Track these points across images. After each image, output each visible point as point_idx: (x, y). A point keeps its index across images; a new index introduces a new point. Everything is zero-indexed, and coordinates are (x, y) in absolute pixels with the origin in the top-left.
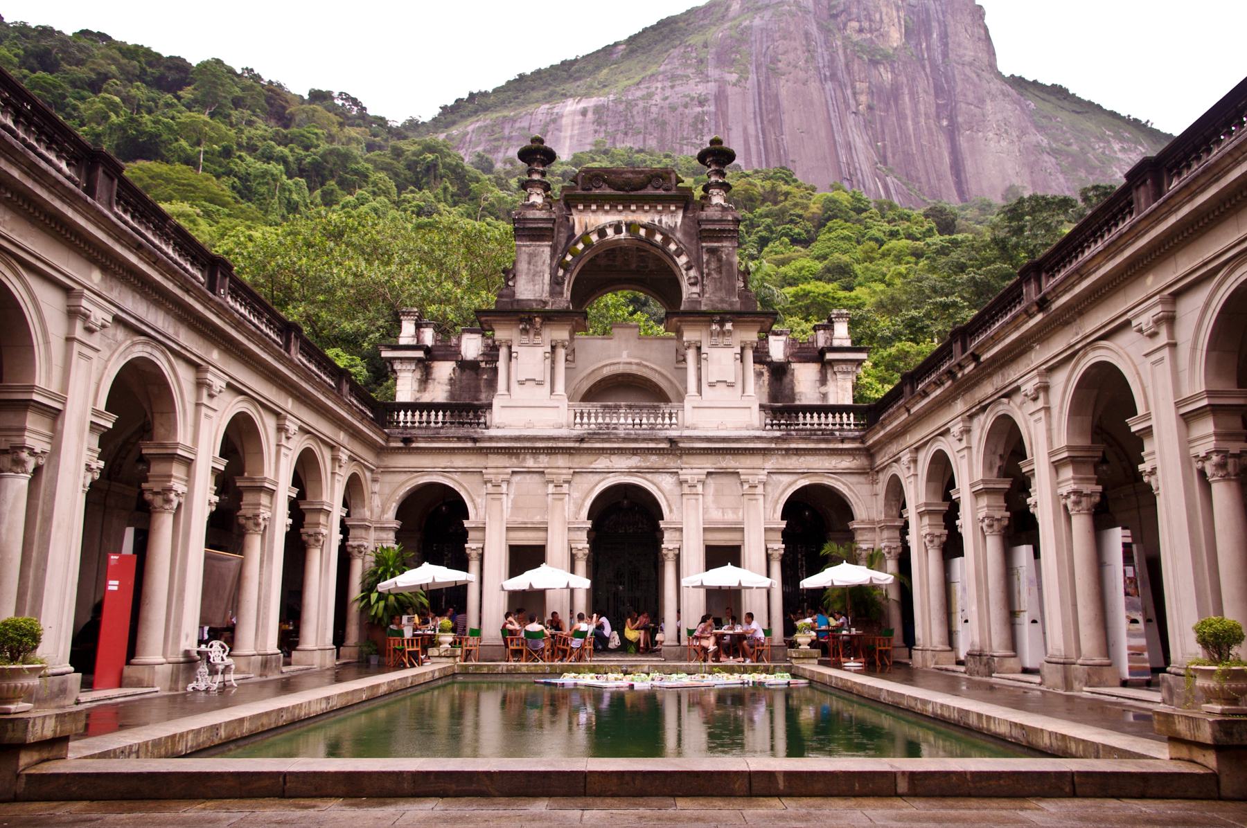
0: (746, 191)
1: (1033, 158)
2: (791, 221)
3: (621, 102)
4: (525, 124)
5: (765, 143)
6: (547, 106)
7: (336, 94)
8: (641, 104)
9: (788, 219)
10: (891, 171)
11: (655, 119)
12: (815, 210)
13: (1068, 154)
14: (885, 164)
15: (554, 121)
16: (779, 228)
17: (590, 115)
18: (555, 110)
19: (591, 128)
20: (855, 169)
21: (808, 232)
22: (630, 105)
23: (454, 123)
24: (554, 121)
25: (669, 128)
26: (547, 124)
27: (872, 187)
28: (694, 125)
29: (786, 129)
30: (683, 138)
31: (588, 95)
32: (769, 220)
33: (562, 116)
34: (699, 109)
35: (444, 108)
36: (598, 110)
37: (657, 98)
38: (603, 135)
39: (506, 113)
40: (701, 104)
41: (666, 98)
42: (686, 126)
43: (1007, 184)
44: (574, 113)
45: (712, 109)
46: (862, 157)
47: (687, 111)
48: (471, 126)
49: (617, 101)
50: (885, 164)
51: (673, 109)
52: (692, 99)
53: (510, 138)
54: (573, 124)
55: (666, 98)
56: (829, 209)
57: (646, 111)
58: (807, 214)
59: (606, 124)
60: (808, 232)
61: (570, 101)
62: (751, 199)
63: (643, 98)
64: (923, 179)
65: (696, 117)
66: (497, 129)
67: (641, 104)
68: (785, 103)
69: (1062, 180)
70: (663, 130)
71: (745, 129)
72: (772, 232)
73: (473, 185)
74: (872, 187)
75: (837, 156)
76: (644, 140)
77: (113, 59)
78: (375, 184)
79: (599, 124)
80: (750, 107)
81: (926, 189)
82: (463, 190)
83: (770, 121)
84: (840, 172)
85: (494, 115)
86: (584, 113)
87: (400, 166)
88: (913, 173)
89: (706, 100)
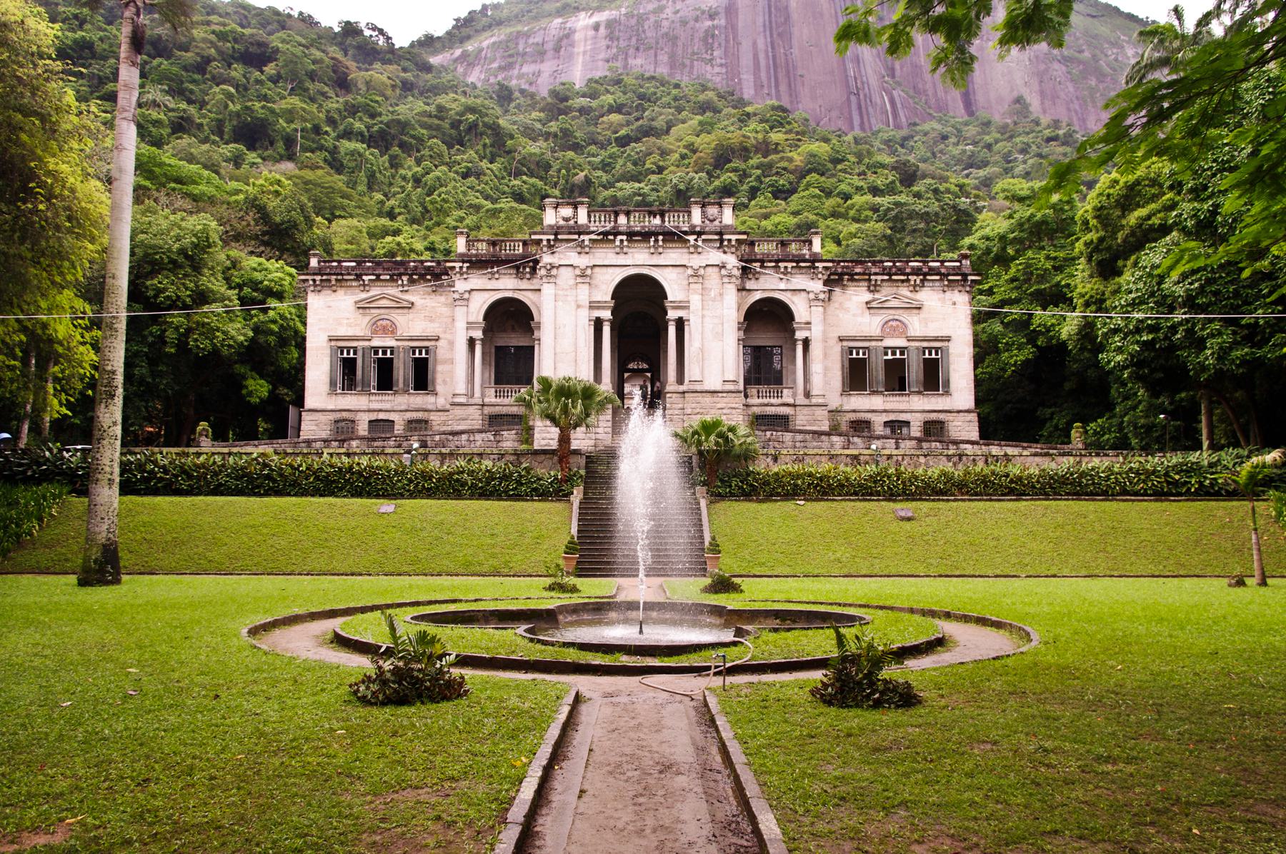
0: (741, 143)
1: (1042, 67)
2: (777, 173)
3: (633, 16)
4: (538, 39)
5: (774, 57)
6: (560, 20)
7: (362, 25)
8: (652, 19)
9: (774, 171)
10: (899, 84)
11: (667, 34)
12: (798, 163)
13: (1080, 62)
14: (893, 76)
15: (567, 36)
16: (767, 179)
17: (602, 30)
18: (568, 25)
19: (604, 43)
20: (863, 83)
21: (791, 183)
22: (641, 19)
23: (469, 37)
24: (567, 36)
25: (680, 43)
26: (560, 40)
27: (878, 101)
28: (705, 40)
29: (795, 42)
30: (694, 53)
31: (599, 9)
32: (759, 172)
33: (575, 31)
34: (709, 23)
35: (457, 20)
36: (610, 24)
37: (669, 11)
38: (615, 50)
39: (519, 28)
40: (712, 17)
41: (677, 12)
42: (696, 40)
43: (1015, 94)
44: (586, 28)
45: (723, 22)
46: (870, 71)
47: (697, 25)
48: (486, 41)
49: (629, 16)
50: (893, 76)
51: (684, 23)
52: (703, 12)
53: (525, 54)
54: (586, 40)
55: (677, 12)
56: (809, 163)
57: (658, 25)
58: (791, 167)
59: (618, 39)
60: (791, 183)
61: (582, 15)
62: (746, 149)
63: (655, 12)
64: (930, 93)
65: (706, 31)
66: (511, 45)
67: (652, 19)
68: (795, 16)
69: (1071, 89)
70: (674, 45)
71: (755, 43)
72: (761, 182)
73: (509, 142)
74: (878, 101)
75: (845, 70)
76: (656, 56)
77: (211, 42)
78: (431, 149)
79: (611, 39)
80: (760, 21)
81: (933, 101)
82: (499, 143)
83: (779, 35)
84: (848, 86)
85: (508, 30)
86: (596, 27)
87: (446, 125)
88: (920, 86)
89: (717, 14)
